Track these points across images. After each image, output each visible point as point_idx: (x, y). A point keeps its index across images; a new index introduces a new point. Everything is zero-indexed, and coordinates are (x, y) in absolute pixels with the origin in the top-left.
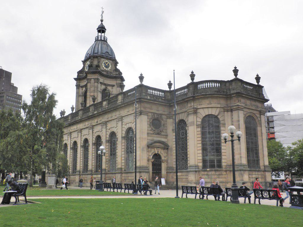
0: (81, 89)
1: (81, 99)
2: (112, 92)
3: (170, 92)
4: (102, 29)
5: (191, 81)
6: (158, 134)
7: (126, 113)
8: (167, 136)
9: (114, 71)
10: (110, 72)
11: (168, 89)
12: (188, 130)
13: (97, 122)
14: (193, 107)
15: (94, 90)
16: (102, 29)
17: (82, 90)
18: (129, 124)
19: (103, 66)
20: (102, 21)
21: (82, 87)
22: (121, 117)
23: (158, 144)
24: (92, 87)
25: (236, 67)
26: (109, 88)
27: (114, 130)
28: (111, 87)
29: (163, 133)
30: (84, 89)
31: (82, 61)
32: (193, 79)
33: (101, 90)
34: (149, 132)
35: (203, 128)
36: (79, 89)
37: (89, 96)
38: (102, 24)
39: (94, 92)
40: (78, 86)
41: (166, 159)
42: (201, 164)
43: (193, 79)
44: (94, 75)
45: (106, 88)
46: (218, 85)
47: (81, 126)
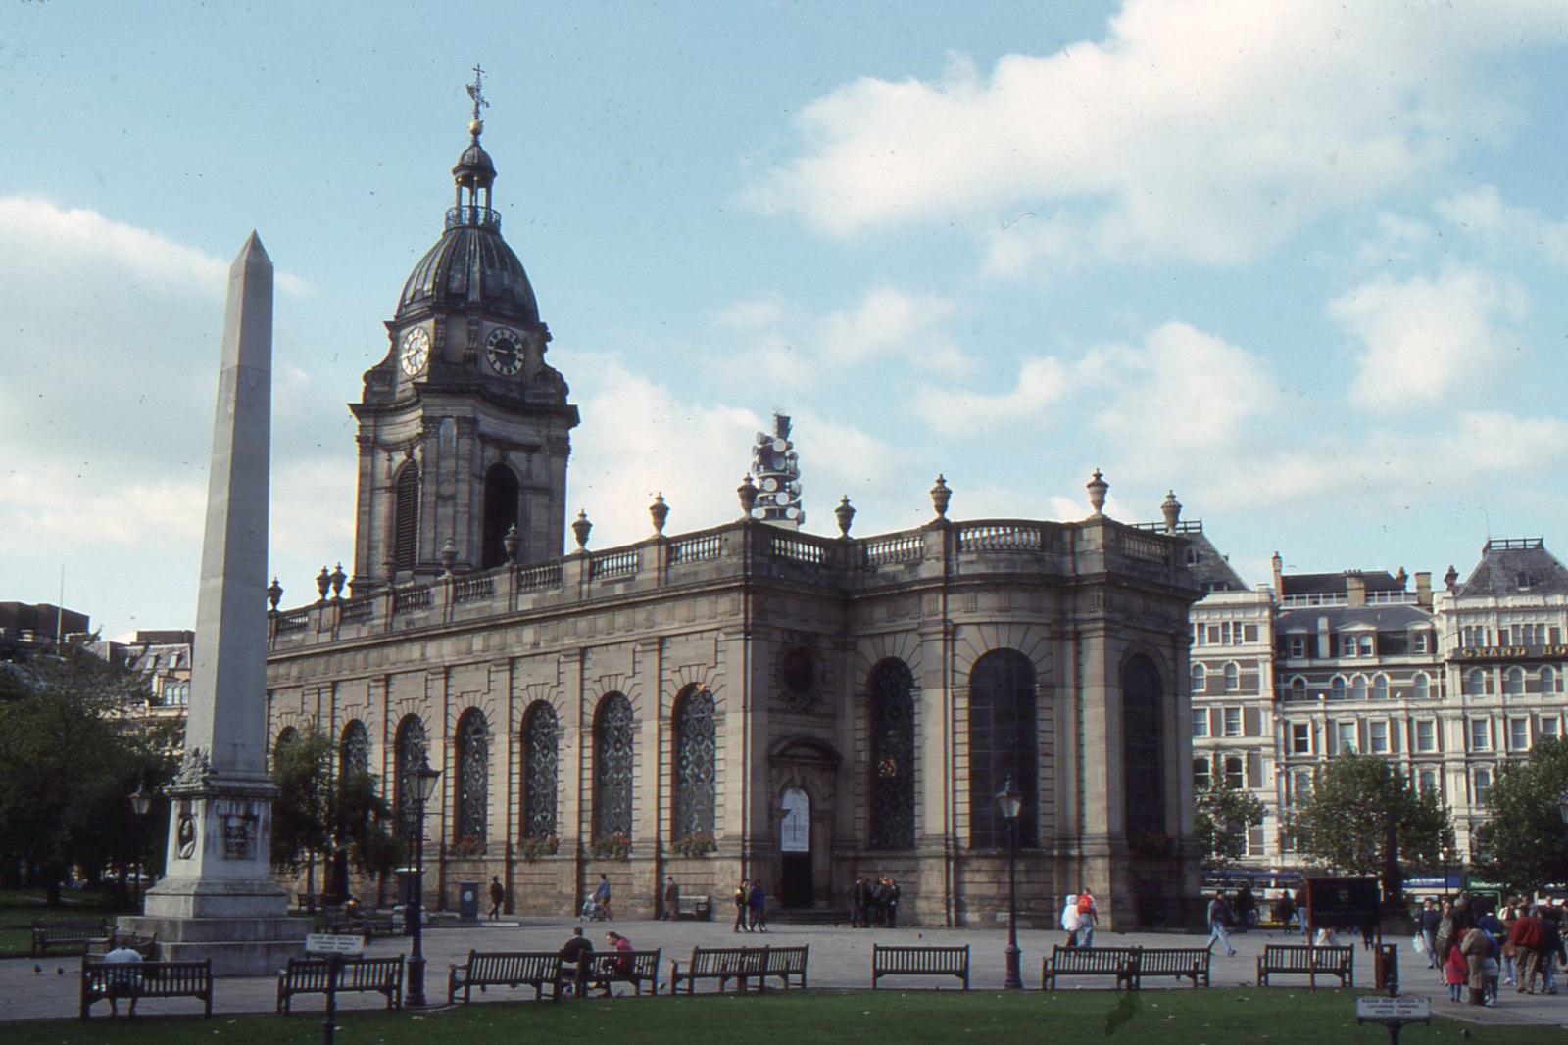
0: (383, 456)
1: (383, 505)
2: (529, 474)
3: (845, 543)
4: (477, 171)
5: (936, 516)
6: (807, 711)
7: (676, 625)
8: (833, 716)
9: (535, 379)
10: (520, 385)
11: (835, 533)
12: (919, 700)
13: (536, 645)
14: (941, 617)
15: (456, 473)
16: (477, 171)
17: (390, 460)
18: (694, 669)
19: (492, 357)
20: (477, 132)
21: (391, 448)
22: (656, 640)
23: (802, 751)
24: (445, 459)
25: (1101, 472)
26: (517, 459)
27: (623, 686)
28: (524, 455)
29: (820, 709)
30: (400, 458)
31: (388, 324)
32: (942, 508)
33: (483, 466)
34: (776, 704)
35: (975, 696)
36: (373, 456)
37: (434, 498)
38: (476, 144)
39: (457, 481)
40: (369, 445)
41: (828, 806)
42: (964, 833)
43: (942, 508)
44: (455, 401)
45: (504, 458)
46: (1034, 537)
47: (443, 651)
